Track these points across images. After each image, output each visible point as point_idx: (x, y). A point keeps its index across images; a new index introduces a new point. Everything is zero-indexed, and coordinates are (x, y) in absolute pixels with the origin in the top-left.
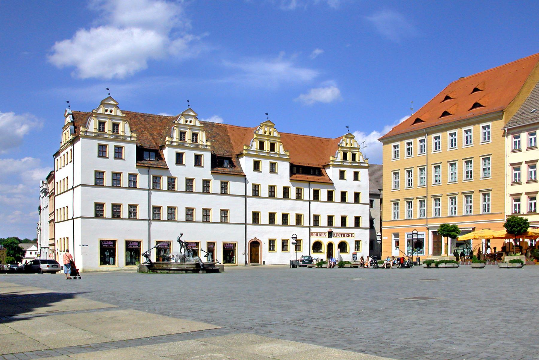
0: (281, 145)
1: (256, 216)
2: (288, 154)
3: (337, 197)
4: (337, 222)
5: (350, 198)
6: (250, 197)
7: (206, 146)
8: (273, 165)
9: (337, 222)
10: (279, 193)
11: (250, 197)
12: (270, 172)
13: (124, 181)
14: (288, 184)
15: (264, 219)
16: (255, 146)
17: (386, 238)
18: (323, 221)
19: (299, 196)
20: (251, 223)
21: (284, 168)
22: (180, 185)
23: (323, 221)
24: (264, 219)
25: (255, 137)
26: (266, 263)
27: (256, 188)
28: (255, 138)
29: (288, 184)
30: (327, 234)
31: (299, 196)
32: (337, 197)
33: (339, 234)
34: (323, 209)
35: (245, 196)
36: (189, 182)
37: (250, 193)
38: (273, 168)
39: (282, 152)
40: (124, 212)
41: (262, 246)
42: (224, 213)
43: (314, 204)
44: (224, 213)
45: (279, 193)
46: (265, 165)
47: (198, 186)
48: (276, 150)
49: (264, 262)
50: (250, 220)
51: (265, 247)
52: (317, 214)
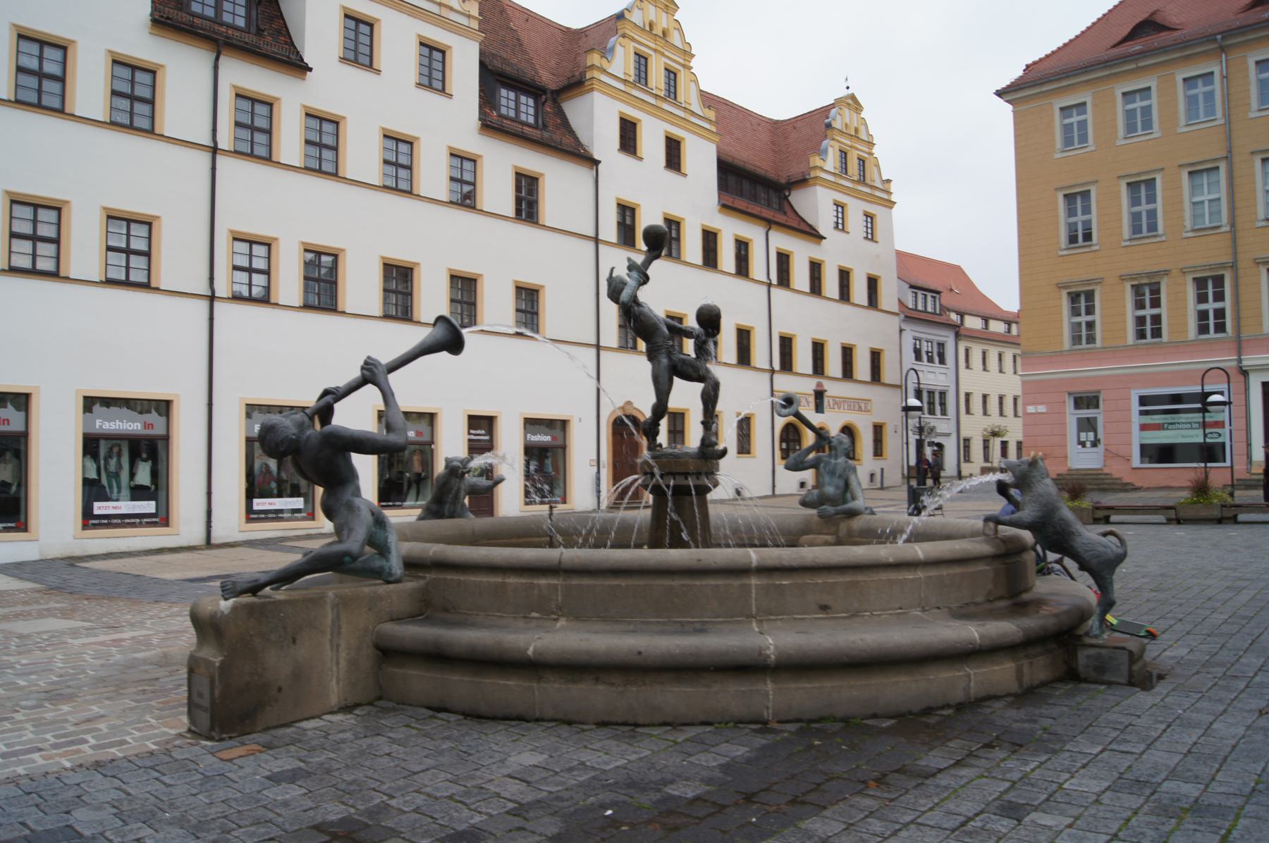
2: (711, 114)
3: (831, 284)
4: (833, 364)
5: (859, 291)
9: (833, 364)
13: (90, 89)
17: (1042, 409)
18: (802, 358)
19: (742, 268)
20: (615, 344)
21: (701, 158)
22: (362, 155)
23: (802, 358)
30: (812, 399)
31: (742, 268)
32: (831, 284)
33: (839, 402)
34: (804, 317)
36: (399, 153)
37: (609, 231)
38: (673, 155)
40: (85, 248)
42: (528, 301)
43: (777, 293)
44: (528, 301)
47: (433, 174)
52: (787, 331)
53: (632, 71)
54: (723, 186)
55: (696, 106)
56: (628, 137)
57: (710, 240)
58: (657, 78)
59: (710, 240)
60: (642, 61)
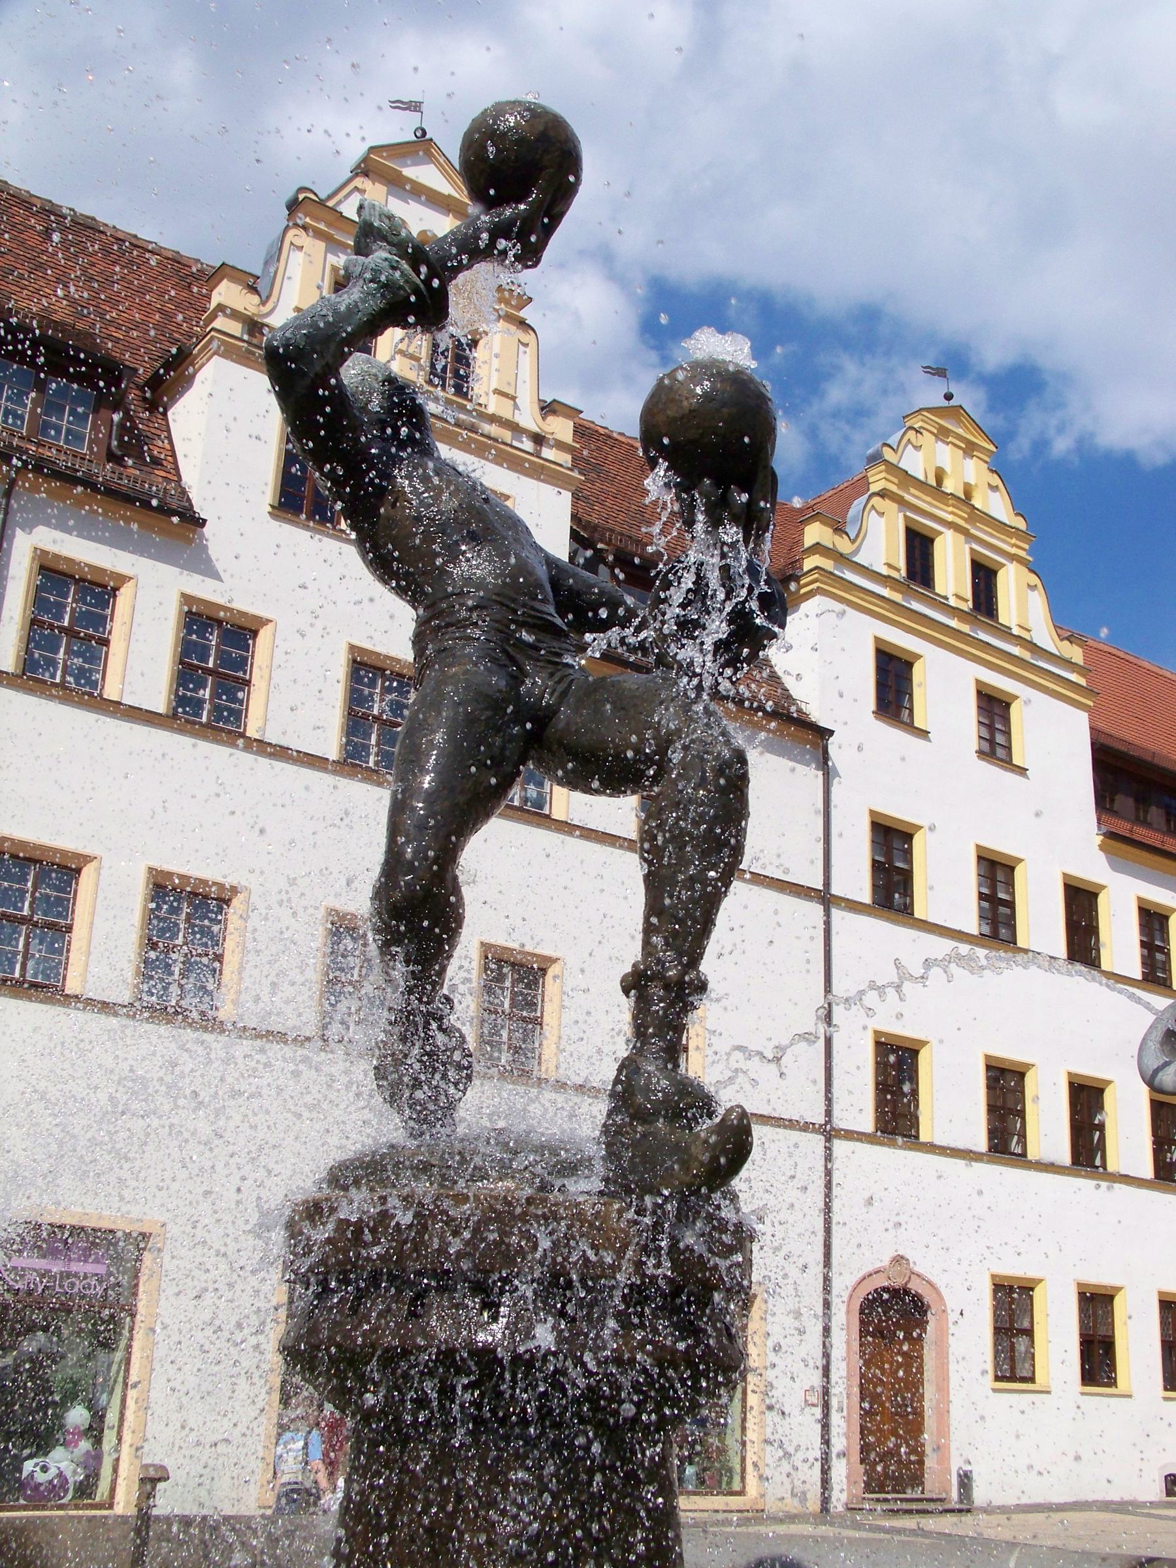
0: (1032, 588)
1: (897, 1064)
2: (1076, 654)
6: (854, 906)
7: (539, 439)
8: (993, 707)
10: (1041, 919)
11: (854, 906)
12: (981, 753)
14: (1094, 866)
15: (952, 1104)
16: (881, 543)
20: (867, 1123)
21: (1057, 738)
24: (952, 1104)
25: (874, 488)
26: (981, 1494)
27: (892, 841)
28: (883, 494)
29: (1094, 866)
35: (826, 898)
37: (855, 877)
39: (1044, 636)
41: (943, 1333)
45: (1041, 919)
46: (946, 685)
48: (1008, 610)
49: (965, 1481)
50: (858, 1106)
51: (963, 1339)
53: (902, 563)
54: (1104, 800)
55: (1044, 636)
56: (893, 683)
57: (1081, 902)
58: (952, 574)
59: (1081, 902)
60: (919, 546)
